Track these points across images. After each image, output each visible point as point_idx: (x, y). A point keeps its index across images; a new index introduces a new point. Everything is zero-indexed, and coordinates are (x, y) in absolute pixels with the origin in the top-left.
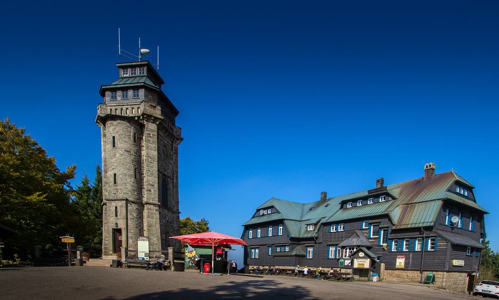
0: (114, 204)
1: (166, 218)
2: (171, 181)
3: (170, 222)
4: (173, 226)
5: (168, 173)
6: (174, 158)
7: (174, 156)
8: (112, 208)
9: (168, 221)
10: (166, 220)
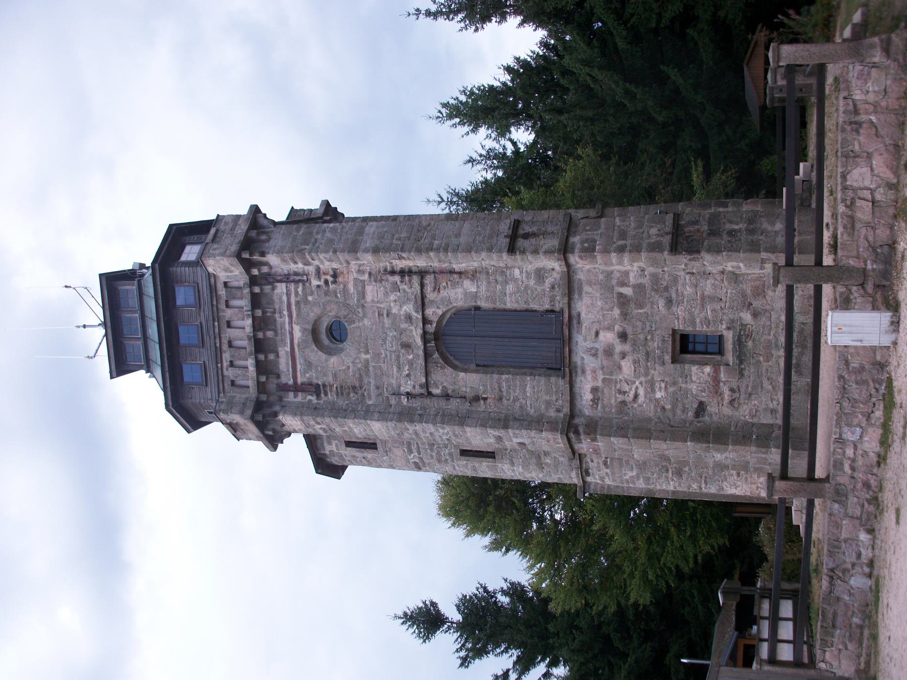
1: (609, 352)
6: (327, 266)
10: (619, 348)
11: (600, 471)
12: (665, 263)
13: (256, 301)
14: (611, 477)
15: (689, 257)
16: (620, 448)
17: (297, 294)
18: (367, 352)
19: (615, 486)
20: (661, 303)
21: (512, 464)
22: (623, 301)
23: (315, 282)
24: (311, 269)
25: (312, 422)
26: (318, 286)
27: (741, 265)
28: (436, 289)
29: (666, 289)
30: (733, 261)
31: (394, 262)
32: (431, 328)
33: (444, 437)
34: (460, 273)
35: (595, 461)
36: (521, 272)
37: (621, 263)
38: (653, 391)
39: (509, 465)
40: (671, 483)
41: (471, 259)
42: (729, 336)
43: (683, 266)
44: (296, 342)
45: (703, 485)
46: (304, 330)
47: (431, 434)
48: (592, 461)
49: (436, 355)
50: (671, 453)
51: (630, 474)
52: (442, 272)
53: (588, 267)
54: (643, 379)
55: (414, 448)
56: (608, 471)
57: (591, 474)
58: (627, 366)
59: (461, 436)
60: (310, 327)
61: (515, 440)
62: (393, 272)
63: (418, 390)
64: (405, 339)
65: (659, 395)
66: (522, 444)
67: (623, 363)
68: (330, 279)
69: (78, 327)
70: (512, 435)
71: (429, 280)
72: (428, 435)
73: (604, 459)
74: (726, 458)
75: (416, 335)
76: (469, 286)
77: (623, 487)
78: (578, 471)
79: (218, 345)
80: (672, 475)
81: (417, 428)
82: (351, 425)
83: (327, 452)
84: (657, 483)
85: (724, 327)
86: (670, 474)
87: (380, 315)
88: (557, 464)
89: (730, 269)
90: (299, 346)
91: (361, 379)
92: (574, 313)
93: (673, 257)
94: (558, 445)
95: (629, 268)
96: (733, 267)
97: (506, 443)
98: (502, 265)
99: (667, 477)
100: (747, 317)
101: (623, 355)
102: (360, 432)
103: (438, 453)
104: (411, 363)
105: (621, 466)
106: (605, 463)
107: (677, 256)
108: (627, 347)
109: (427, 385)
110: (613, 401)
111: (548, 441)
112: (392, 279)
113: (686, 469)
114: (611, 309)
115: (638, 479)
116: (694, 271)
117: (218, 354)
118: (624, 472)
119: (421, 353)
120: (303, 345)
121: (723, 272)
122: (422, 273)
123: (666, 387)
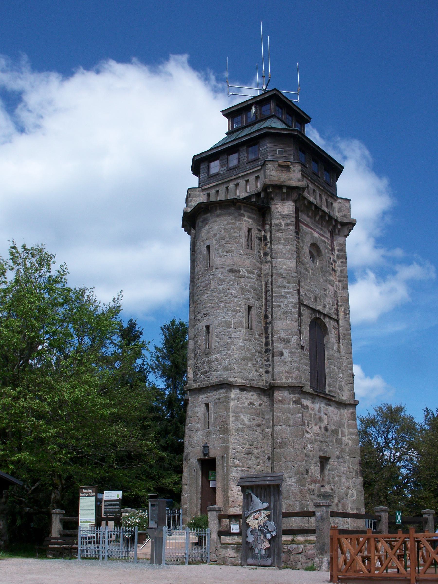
0: (202, 398)
1: (321, 419)
2: (333, 323)
3: (333, 431)
4: (339, 442)
5: (325, 307)
6: (338, 269)
7: (339, 263)
8: (198, 409)
9: (326, 429)
10: (323, 426)
11: (246, 399)
12: (352, 457)
14: (239, 405)
15: (358, 470)
16: (288, 419)
18: (313, 274)
19: (230, 407)
20: (337, 453)
21: (244, 340)
22: (336, 432)
25: (287, 221)
27: (354, 498)
29: (342, 457)
30: (356, 493)
31: (343, 307)
32: (322, 317)
34: (339, 343)
35: (252, 397)
37: (350, 433)
38: (311, 443)
39: (243, 337)
40: (240, 447)
41: (347, 352)
43: (351, 467)
45: (240, 469)
46: (316, 238)
48: (252, 395)
50: (289, 450)
51: (246, 420)
53: (345, 415)
54: (313, 438)
55: (250, 275)
57: (241, 392)
58: (316, 429)
59: (286, 317)
61: (286, 352)
63: (301, 298)
64: (318, 300)
65: (309, 446)
66: (281, 354)
72: (283, 294)
73: (254, 403)
74: (291, 485)
77: (229, 412)
78: (248, 384)
79: (316, 183)
80: (248, 448)
81: (291, 290)
82: (288, 247)
83: (242, 212)
84: (238, 437)
85: (333, 487)
86: (249, 447)
87: (325, 290)
88: (249, 371)
89: (350, 492)
90: (311, 232)
92: (331, 403)
93: (357, 462)
94: (284, 378)
95: (347, 438)
96: (352, 493)
97: (282, 344)
98: (343, 368)
100: (336, 501)
101: (320, 428)
105: (251, 414)
106: (251, 404)
107: (359, 465)
108: (323, 430)
111: (288, 372)
112: (335, 302)
113: (253, 458)
115: (241, 424)
116: (348, 473)
118: (247, 415)
119: (314, 307)
120: (313, 237)
121: (349, 488)
122: (337, 321)
123: (311, 451)
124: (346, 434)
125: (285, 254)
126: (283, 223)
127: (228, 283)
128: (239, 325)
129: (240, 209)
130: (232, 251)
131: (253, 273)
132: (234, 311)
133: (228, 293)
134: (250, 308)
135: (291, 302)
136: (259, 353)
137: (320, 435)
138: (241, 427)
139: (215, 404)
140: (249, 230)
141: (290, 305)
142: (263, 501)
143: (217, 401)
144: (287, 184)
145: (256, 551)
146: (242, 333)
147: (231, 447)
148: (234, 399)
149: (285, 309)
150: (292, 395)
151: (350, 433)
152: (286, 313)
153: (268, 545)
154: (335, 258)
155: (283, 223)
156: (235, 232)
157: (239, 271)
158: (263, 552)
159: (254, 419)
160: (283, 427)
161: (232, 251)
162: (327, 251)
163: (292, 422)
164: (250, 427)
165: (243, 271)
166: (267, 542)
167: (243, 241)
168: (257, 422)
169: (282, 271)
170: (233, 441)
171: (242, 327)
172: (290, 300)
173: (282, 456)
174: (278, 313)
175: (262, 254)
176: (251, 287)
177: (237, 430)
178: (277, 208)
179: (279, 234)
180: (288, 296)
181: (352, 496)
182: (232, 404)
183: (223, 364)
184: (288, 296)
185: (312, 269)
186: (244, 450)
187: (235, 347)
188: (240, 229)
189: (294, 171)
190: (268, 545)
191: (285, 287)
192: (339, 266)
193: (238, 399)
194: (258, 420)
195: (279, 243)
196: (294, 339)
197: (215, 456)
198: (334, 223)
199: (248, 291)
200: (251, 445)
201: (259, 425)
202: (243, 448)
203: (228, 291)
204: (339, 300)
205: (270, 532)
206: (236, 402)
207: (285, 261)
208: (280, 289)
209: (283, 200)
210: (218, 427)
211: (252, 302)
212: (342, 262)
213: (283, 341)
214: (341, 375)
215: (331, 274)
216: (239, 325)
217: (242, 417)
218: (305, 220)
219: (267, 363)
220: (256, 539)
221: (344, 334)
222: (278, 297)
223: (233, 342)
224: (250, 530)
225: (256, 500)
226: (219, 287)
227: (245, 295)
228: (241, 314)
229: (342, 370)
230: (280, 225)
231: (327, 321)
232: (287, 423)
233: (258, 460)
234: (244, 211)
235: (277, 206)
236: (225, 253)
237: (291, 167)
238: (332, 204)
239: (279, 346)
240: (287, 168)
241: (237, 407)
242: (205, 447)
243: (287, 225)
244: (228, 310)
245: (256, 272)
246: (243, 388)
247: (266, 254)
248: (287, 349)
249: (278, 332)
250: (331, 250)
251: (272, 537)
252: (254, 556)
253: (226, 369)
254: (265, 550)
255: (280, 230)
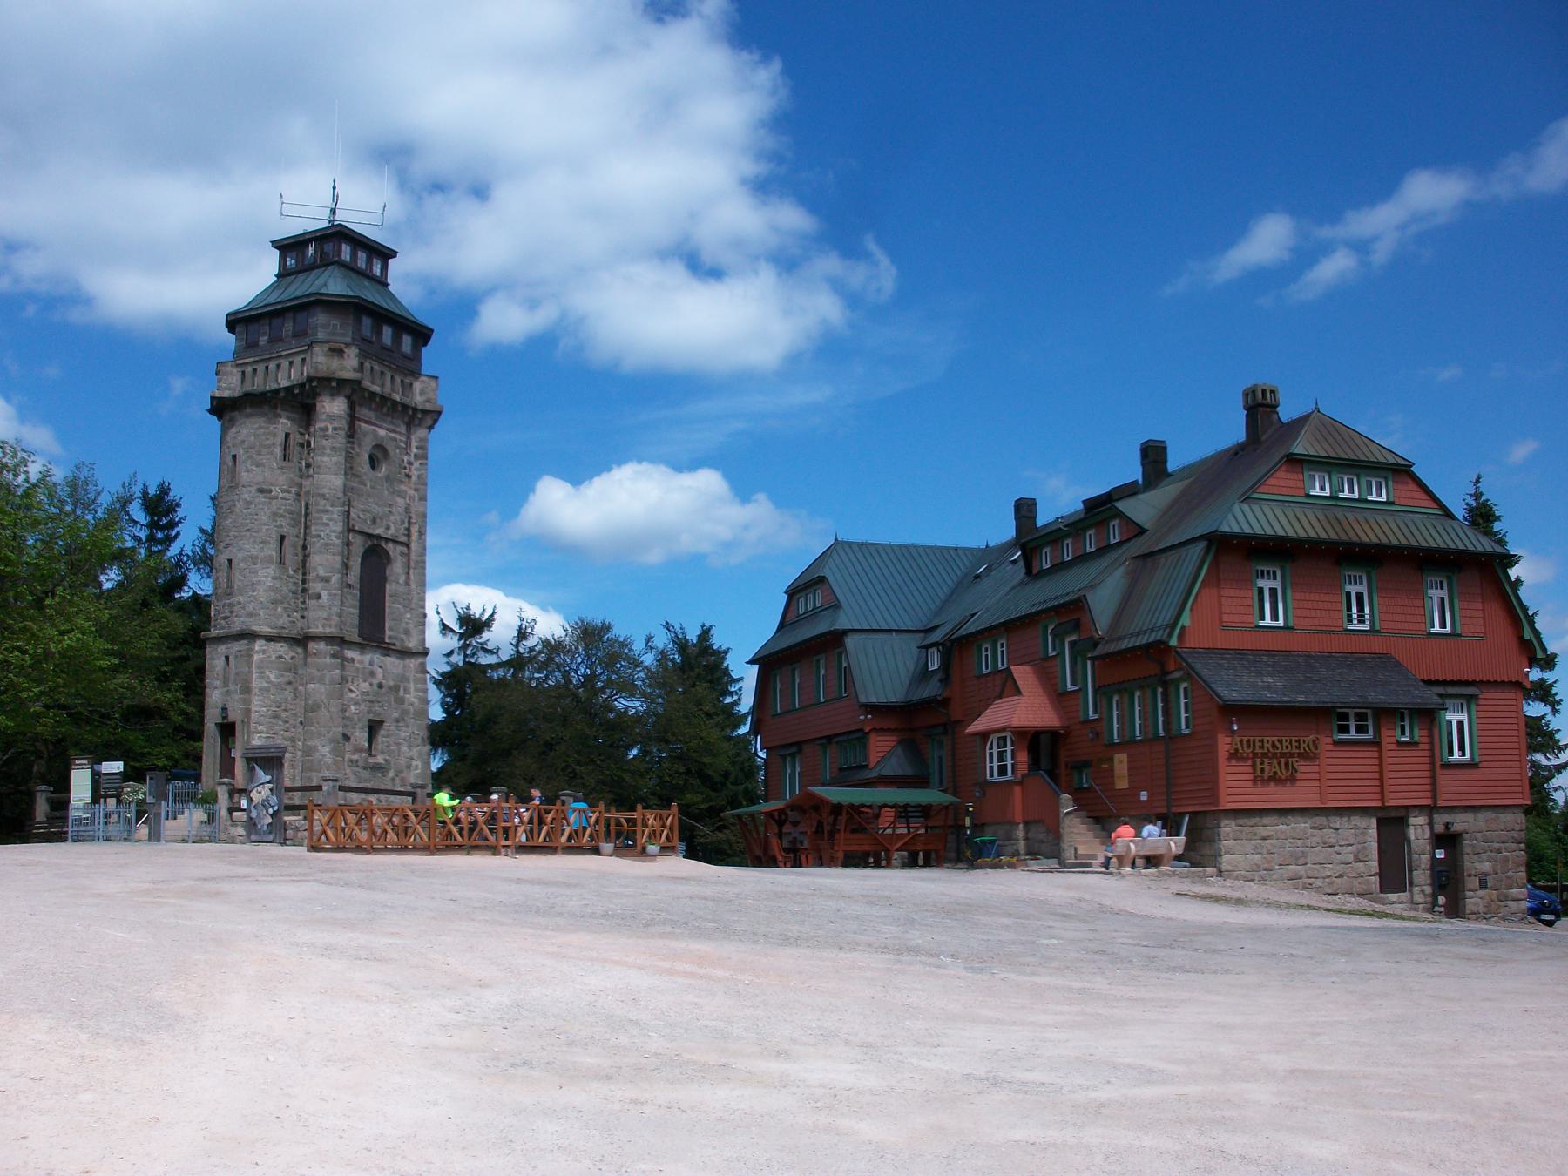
0: (222, 649)
1: (372, 674)
2: (401, 548)
3: (390, 688)
5: (388, 528)
6: (414, 474)
7: (417, 464)
9: (380, 686)
10: (375, 682)
13: (405, 407)
15: (425, 737)
17: (401, 441)
18: (372, 487)
20: (396, 715)
21: (274, 578)
22: (396, 688)
23: (406, 458)
24: (412, 459)
25: (336, 424)
26: (403, 461)
27: (419, 771)
28: (402, 554)
29: (404, 720)
32: (383, 544)
33: (322, 534)
34: (408, 573)
36: (408, 619)
38: (355, 704)
40: (264, 709)
42: (380, 759)
43: (416, 732)
44: (377, 429)
45: (264, 735)
46: (383, 438)
47: (327, 525)
48: (282, 647)
49: (370, 543)
50: (323, 713)
51: (272, 677)
52: (409, 560)
53: (412, 665)
54: (359, 697)
55: (286, 495)
56: (274, 657)
58: (365, 686)
60: (384, 444)
61: (324, 594)
62: (409, 522)
63: (351, 522)
64: (378, 520)
65: (352, 707)
66: (319, 597)
67: (367, 684)
68: (407, 471)
69: (334, 181)
70: (334, 592)
71: (404, 549)
72: (325, 521)
74: (324, 756)
75: (378, 531)
76: (402, 580)
77: (252, 667)
81: (335, 516)
83: (279, 411)
87: (390, 505)
89: (414, 763)
90: (374, 430)
91: (358, 476)
92: (390, 652)
93: (425, 726)
96: (416, 766)
98: (413, 606)
99: (271, 706)
100: (391, 774)
101: (371, 684)
102: (323, 461)
103: (282, 516)
104: (365, 521)
105: (279, 669)
106: (280, 657)
108: (375, 687)
109: (355, 531)
110: (348, 673)
111: (325, 619)
112: (406, 520)
113: (280, 723)
114: (393, 680)
117: (380, 361)
119: (371, 531)
120: (376, 435)
122: (407, 545)
123: (356, 714)
124: (412, 690)
125: (329, 468)
126: (330, 427)
127: (256, 506)
128: (268, 560)
129: (275, 407)
130: (262, 465)
131: (289, 492)
132: (262, 542)
133: (256, 520)
134: (283, 538)
135: (334, 532)
136: (293, 593)
137: (371, 693)
138: (266, 685)
139: (236, 657)
140: (287, 435)
141: (333, 534)
142: (266, 774)
143: (238, 653)
144: (336, 376)
145: (259, 827)
146: (272, 570)
147: (253, 709)
148: (258, 652)
149: (326, 541)
150: (329, 647)
151: (416, 690)
152: (327, 544)
153: (270, 821)
154: (412, 459)
155: (330, 427)
156: (268, 439)
157: (271, 491)
158: (265, 828)
159: (282, 676)
160: (317, 685)
161: (262, 465)
162: (398, 451)
163: (327, 681)
164: (277, 686)
165: (276, 491)
166: (269, 817)
167: (278, 451)
168: (287, 679)
169: (325, 491)
170: (256, 703)
171: (272, 563)
172: (334, 528)
173: (314, 721)
174: (315, 546)
175: (304, 464)
176: (285, 510)
177: (261, 689)
178: (324, 407)
179: (324, 442)
180: (331, 523)
181: (416, 769)
182: (256, 657)
183: (247, 608)
184: (331, 523)
185: (371, 481)
186: (270, 713)
187: (261, 588)
188: (275, 435)
189: (348, 356)
190: (270, 821)
191: (327, 511)
192: (416, 469)
193: (264, 652)
194: (289, 676)
195: (323, 454)
196: (335, 578)
197: (234, 720)
198: (411, 412)
199: (282, 516)
200: (278, 707)
201: (290, 683)
202: (268, 710)
203: (256, 517)
204: (413, 515)
205: (272, 807)
206: (261, 656)
207: (328, 477)
208: (322, 515)
209: (332, 395)
210: (239, 686)
211: (286, 530)
212: (421, 464)
213: (322, 580)
214: (408, 616)
215: (402, 482)
216: (268, 560)
217: (268, 673)
218: (366, 416)
219: (303, 606)
220: (259, 814)
221: (417, 561)
222: (317, 524)
223: (259, 581)
224: (254, 804)
225: (260, 772)
226: (245, 511)
227: (276, 521)
228: (271, 546)
229: (412, 609)
230: (326, 429)
231: (390, 547)
232: (321, 680)
233: (287, 725)
234: (282, 410)
235: (324, 404)
236: (254, 468)
237: (346, 350)
238: (411, 384)
239: (314, 587)
240: (338, 352)
241: (262, 661)
242: (224, 709)
243: (335, 429)
244: (255, 542)
245: (293, 490)
246: (270, 639)
247: (308, 466)
248: (325, 590)
249: (315, 569)
250: (406, 449)
251: (274, 812)
252: (257, 833)
253: (250, 615)
254: (268, 825)
255: (325, 437)
